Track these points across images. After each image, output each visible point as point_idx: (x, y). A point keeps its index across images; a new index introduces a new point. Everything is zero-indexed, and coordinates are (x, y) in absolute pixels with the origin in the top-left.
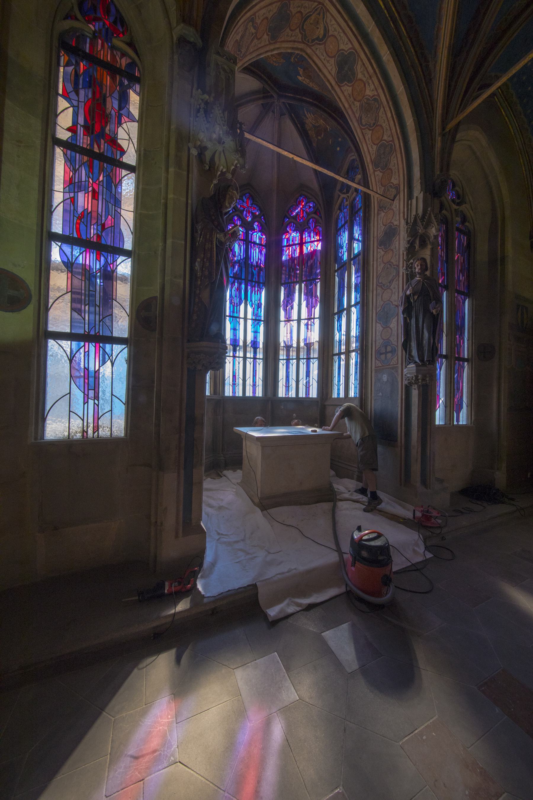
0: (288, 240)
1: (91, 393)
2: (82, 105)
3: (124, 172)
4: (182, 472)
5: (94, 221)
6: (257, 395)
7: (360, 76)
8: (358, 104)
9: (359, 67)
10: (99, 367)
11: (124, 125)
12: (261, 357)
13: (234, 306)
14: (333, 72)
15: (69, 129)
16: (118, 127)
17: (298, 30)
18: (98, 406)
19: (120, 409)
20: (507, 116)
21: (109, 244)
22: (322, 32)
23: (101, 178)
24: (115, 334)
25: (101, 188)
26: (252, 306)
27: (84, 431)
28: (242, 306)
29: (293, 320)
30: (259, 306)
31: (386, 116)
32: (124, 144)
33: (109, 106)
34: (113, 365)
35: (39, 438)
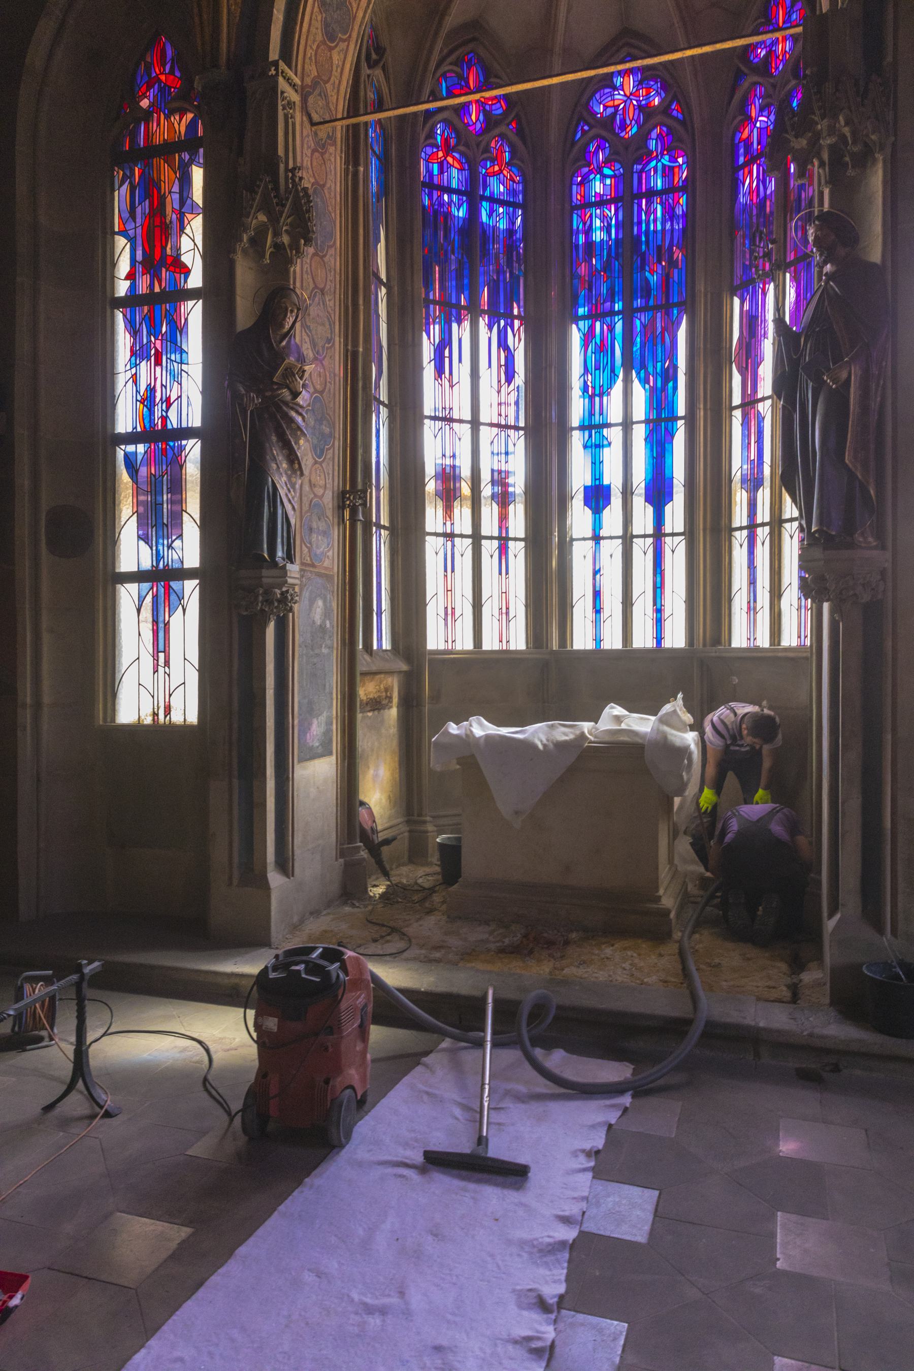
0: (748, 142)
3: (190, 303)
6: (667, 644)
10: (170, 617)
12: (680, 528)
13: (592, 398)
15: (127, 278)
16: (180, 236)
18: (169, 675)
21: (175, 426)
23: (164, 330)
26: (647, 381)
27: (154, 713)
30: (670, 375)
32: (186, 259)
33: (169, 210)
35: (109, 720)
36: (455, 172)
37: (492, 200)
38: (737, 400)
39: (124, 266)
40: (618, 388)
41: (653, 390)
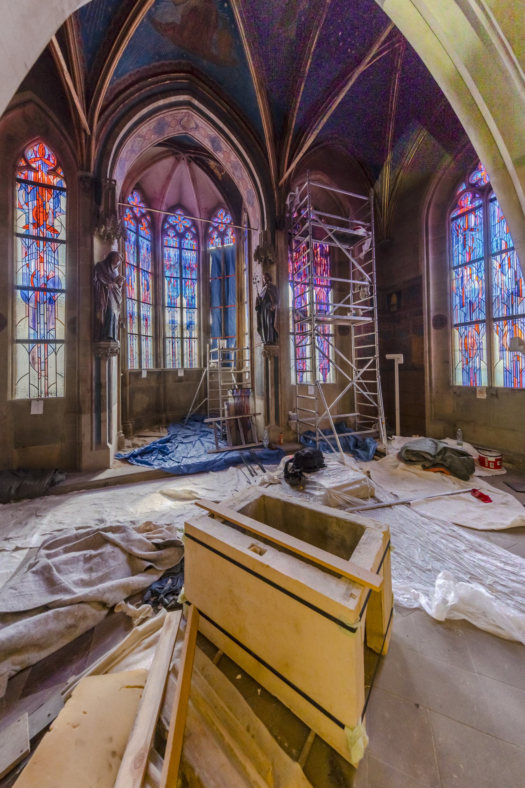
8: (230, 164)
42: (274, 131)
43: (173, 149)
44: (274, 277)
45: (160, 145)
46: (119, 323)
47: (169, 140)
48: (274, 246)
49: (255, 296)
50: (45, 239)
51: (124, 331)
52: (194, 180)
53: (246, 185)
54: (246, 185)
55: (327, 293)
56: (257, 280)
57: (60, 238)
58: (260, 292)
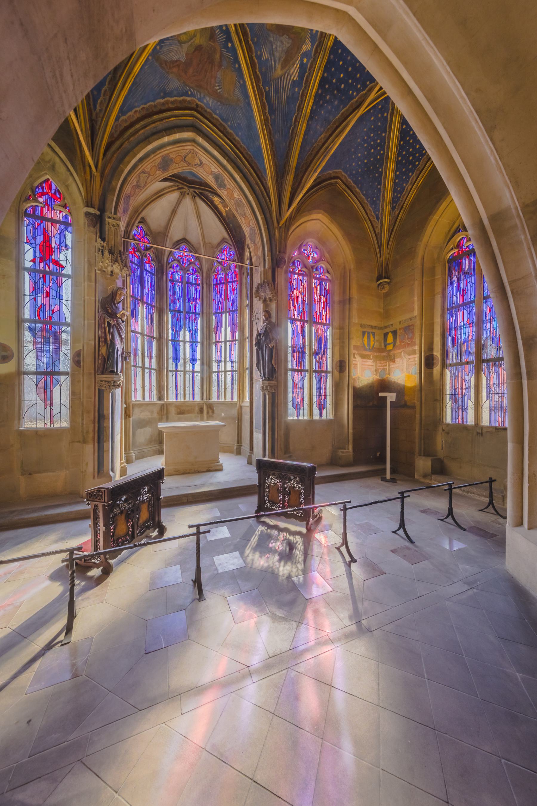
1: (49, 403)
2: (38, 247)
4: (96, 444)
5: (47, 309)
7: (228, 186)
8: (233, 201)
9: (226, 182)
11: (63, 252)
14: (214, 181)
17: (182, 162)
19: (66, 412)
20: (349, 196)
22: (199, 161)
24: (62, 370)
25: (51, 290)
28: (182, 333)
29: (221, 342)
30: (196, 331)
31: (248, 211)
34: (60, 387)
36: (136, 259)
37: (147, 271)
38: (214, 340)
39: (29, 255)
40: (182, 331)
41: (192, 334)
42: (276, 170)
43: (178, 184)
44: (274, 314)
45: (165, 180)
46: (122, 356)
47: (173, 176)
48: (274, 284)
49: (255, 333)
50: (51, 273)
51: (128, 363)
52: (199, 216)
53: (249, 224)
54: (249, 224)
55: (327, 330)
56: (257, 317)
57: (65, 272)
58: (259, 329)
